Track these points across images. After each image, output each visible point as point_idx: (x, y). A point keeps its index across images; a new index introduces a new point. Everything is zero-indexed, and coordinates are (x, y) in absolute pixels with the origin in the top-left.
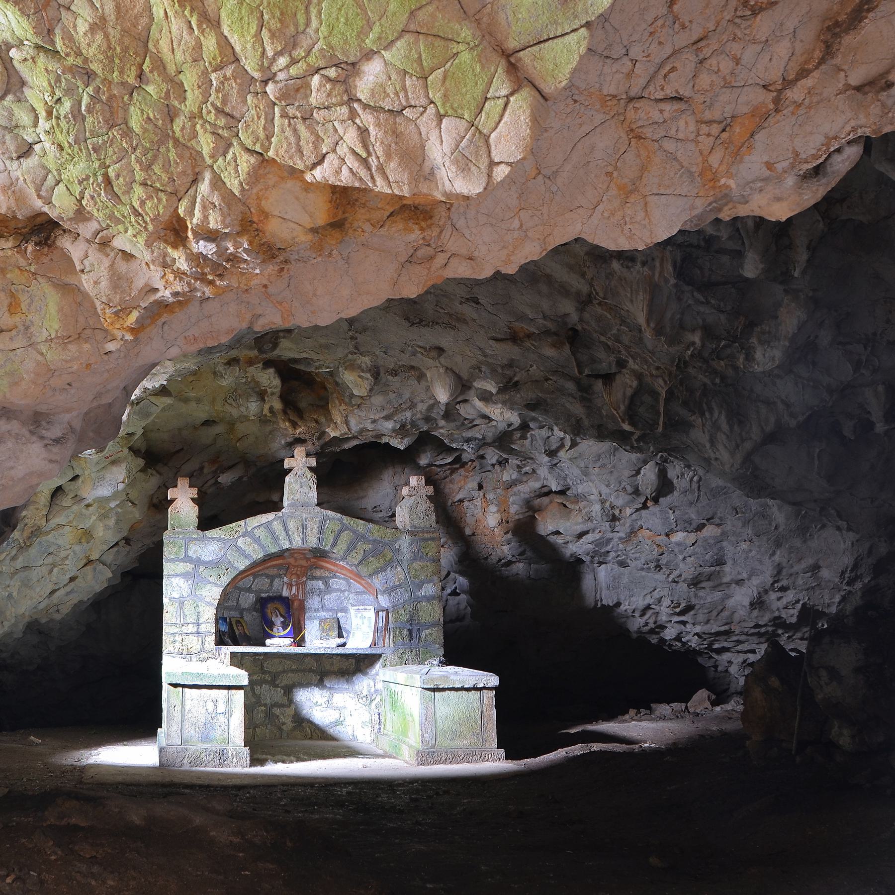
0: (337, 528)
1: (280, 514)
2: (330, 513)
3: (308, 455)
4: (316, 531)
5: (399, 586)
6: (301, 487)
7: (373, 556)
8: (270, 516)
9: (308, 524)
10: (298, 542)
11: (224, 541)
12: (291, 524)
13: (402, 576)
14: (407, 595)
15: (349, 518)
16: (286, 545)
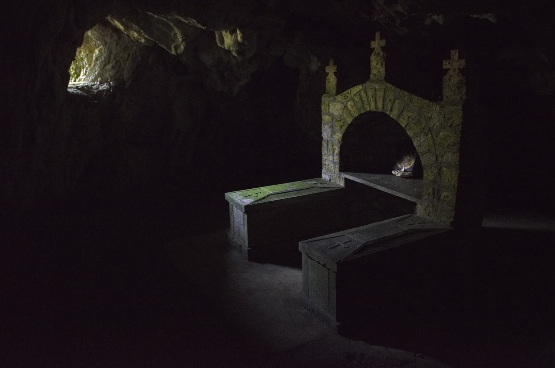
0: (392, 98)
1: (364, 85)
2: (389, 85)
3: (381, 38)
4: (381, 100)
5: (429, 151)
6: (377, 64)
7: (413, 123)
8: (360, 87)
9: (378, 93)
10: (373, 107)
11: (343, 103)
12: (370, 93)
13: (431, 142)
14: (435, 159)
15: (399, 90)
16: (368, 109)
